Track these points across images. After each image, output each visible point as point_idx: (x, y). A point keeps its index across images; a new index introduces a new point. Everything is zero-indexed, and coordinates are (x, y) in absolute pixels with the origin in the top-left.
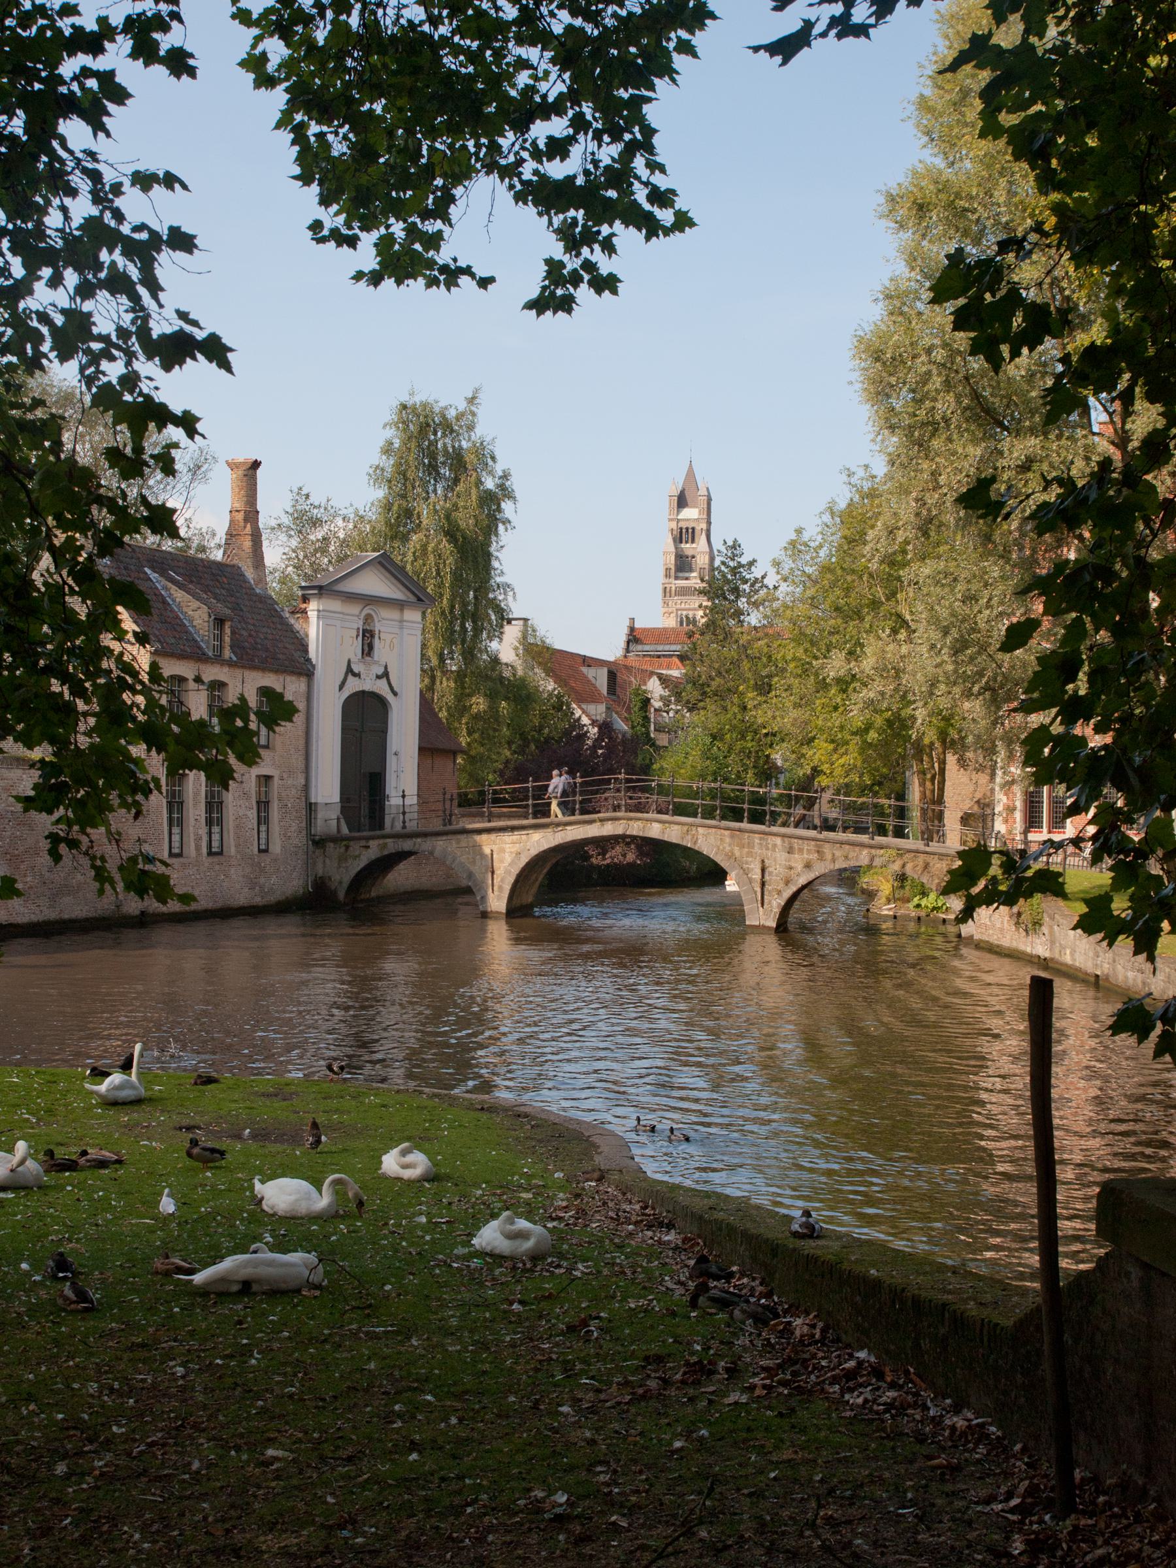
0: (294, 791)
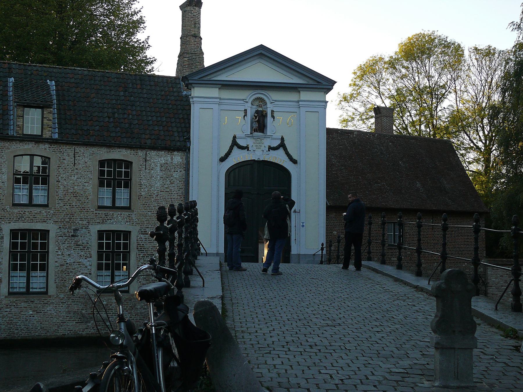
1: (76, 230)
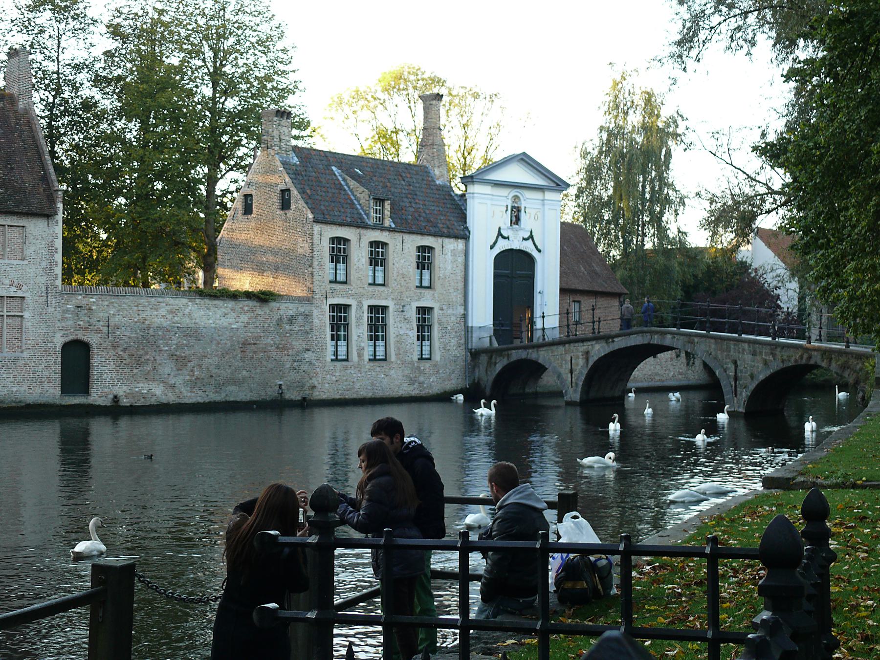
0: (453, 318)
1: (404, 306)
